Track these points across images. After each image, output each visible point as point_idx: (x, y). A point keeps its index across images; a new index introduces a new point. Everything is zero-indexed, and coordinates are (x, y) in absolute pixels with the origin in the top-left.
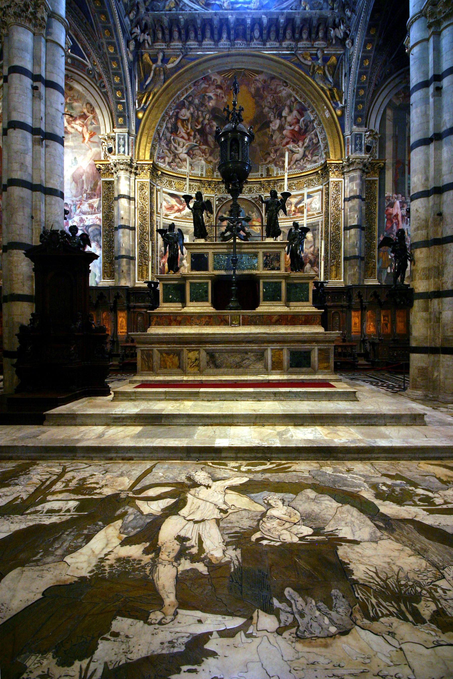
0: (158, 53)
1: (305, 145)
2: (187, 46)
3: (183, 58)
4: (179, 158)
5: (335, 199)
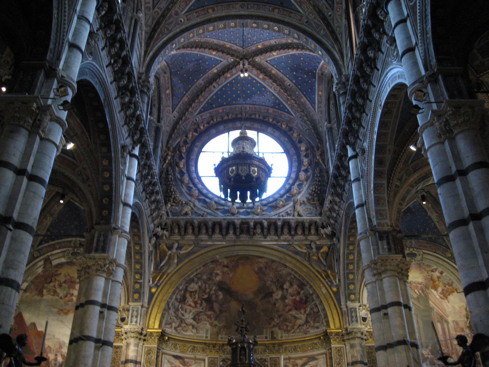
0: (173, 244)
1: (307, 312)
2: (198, 239)
3: (195, 246)
4: (185, 323)
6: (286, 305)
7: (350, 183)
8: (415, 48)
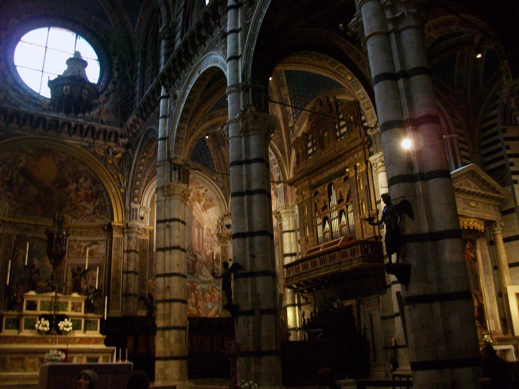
1: (96, 205)
5: (116, 250)
6: (78, 196)
7: (158, 118)
8: (239, 58)
